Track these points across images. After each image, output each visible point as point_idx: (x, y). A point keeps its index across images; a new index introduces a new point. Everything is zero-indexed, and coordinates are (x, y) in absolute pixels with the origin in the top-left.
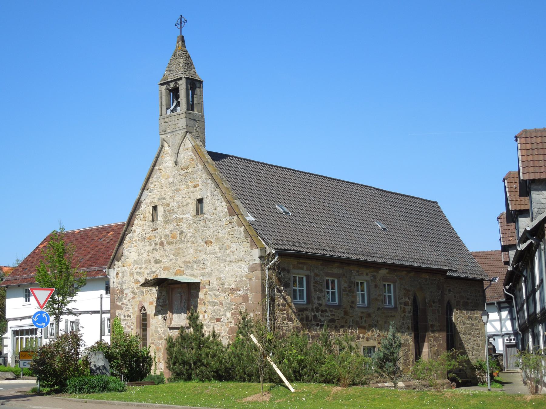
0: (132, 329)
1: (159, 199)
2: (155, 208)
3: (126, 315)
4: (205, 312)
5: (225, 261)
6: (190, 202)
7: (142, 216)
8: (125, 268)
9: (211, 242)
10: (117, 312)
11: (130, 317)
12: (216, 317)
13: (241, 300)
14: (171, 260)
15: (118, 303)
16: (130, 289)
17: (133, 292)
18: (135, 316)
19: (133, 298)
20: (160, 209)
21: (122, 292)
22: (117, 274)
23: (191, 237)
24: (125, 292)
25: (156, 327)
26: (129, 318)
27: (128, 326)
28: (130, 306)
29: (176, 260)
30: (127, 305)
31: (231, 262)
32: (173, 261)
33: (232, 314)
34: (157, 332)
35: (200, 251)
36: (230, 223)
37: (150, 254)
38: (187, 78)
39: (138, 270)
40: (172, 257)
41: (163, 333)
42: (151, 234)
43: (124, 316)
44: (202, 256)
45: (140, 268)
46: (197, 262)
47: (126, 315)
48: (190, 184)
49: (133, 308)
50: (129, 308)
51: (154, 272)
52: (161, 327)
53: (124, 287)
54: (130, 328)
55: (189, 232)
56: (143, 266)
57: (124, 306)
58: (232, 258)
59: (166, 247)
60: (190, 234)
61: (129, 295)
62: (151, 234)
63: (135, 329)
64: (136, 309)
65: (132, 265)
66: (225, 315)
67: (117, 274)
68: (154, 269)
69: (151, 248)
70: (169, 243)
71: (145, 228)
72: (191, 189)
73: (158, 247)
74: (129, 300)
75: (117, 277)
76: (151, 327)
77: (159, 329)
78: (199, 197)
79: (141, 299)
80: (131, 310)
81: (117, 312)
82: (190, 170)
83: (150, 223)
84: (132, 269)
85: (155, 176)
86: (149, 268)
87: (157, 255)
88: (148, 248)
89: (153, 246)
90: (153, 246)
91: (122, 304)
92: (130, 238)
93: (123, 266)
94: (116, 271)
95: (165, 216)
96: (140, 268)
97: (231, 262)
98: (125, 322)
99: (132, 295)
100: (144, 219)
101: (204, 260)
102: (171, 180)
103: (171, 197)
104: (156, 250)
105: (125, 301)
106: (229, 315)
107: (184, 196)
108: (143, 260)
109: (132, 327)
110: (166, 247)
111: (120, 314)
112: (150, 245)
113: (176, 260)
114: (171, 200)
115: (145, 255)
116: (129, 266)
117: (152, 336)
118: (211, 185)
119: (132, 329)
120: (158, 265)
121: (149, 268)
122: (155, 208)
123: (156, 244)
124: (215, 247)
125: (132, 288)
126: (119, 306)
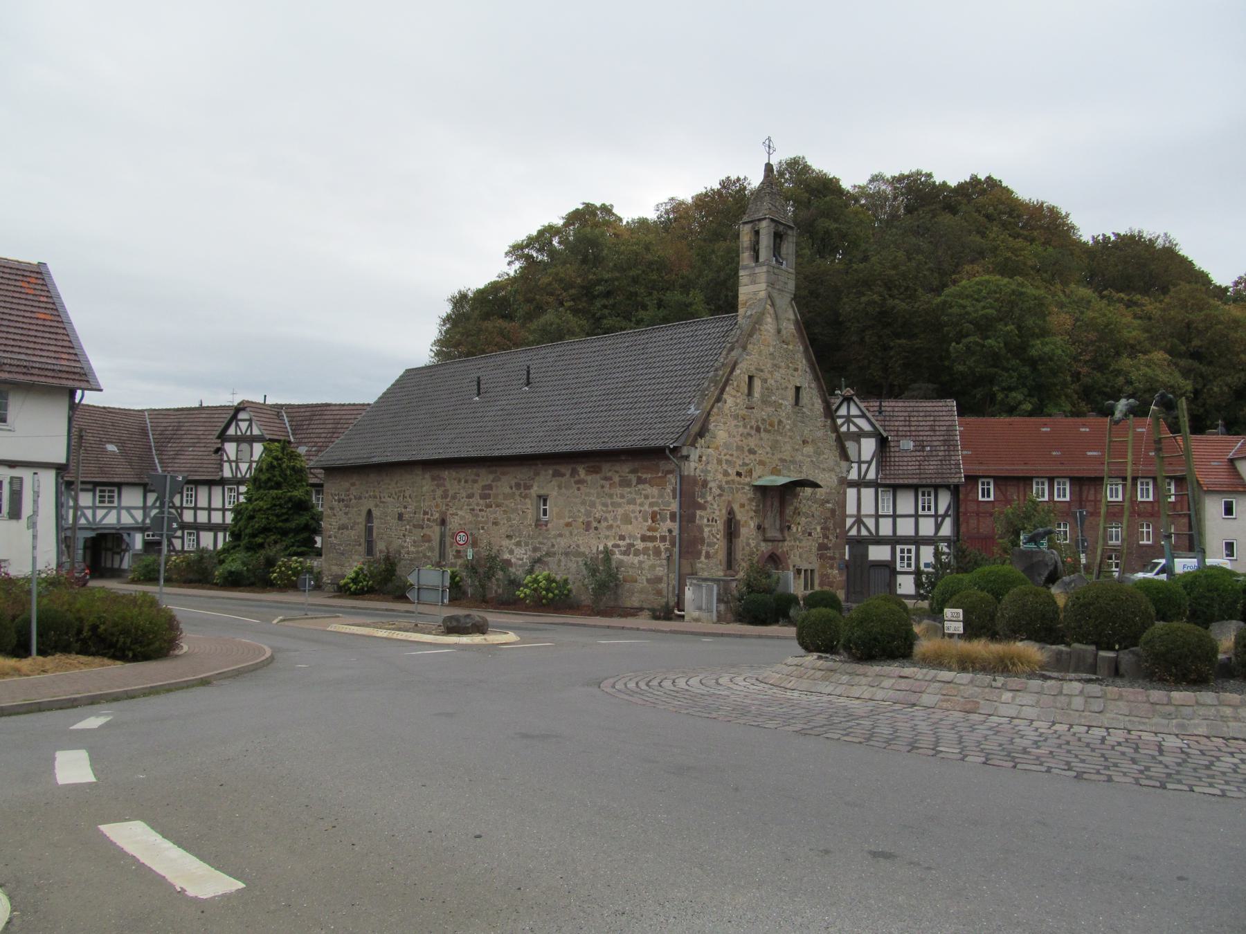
0: (718, 539)
1: (756, 369)
2: (751, 378)
3: (710, 519)
4: (799, 524)
5: (819, 467)
6: (790, 386)
7: (735, 384)
8: (710, 450)
9: (808, 442)
10: (698, 512)
11: (716, 522)
12: (808, 531)
13: (829, 515)
14: (767, 453)
15: (699, 500)
16: (717, 482)
17: (720, 487)
18: (723, 521)
19: (720, 495)
20: (757, 383)
21: (705, 484)
22: (700, 457)
23: (789, 430)
24: (709, 486)
25: (748, 539)
26: (714, 523)
27: (713, 534)
28: (715, 506)
29: (773, 454)
30: (712, 505)
31: (824, 470)
32: (769, 455)
33: (822, 529)
34: (748, 544)
35: (797, 450)
36: (825, 426)
37: (743, 439)
38: (772, 220)
39: (728, 457)
40: (768, 449)
41: (755, 547)
42: (744, 412)
43: (708, 520)
44: (799, 458)
45: (732, 455)
46: (793, 462)
47: (710, 519)
48: (790, 365)
49: (720, 510)
50: (715, 509)
51: (747, 465)
52: (753, 539)
53: (709, 478)
54: (716, 537)
55: (788, 424)
56: (735, 453)
57: (709, 506)
58: (825, 466)
59: (763, 434)
60: (788, 427)
61: (714, 490)
62: (744, 412)
63: (722, 539)
64: (724, 511)
65: (720, 449)
66: (815, 529)
67: (700, 457)
68: (747, 461)
69: (746, 431)
70: (766, 431)
71: (738, 401)
72: (791, 371)
73: (753, 432)
74: (714, 498)
75: (700, 461)
76: (741, 538)
77: (751, 541)
78: (798, 385)
79: (730, 499)
80: (717, 513)
81: (698, 512)
82: (791, 347)
83: (745, 397)
84: (720, 455)
85: (755, 337)
86: (741, 457)
87: (752, 442)
88: (741, 430)
89: (748, 430)
90: (748, 430)
91: (705, 502)
92: (719, 408)
93: (708, 447)
94: (698, 452)
95: (762, 395)
96: (732, 455)
97: (824, 470)
98: (709, 529)
99: (718, 492)
100: (737, 389)
101: (800, 461)
102: (771, 349)
103: (771, 373)
104: (752, 436)
105: (709, 498)
106: (819, 529)
107: (784, 376)
108: (735, 444)
109: (718, 536)
110: (763, 434)
111: (702, 517)
112: (745, 426)
113: (773, 454)
114: (769, 376)
115: (738, 438)
116: (717, 448)
117: (743, 549)
118: (809, 376)
119: (718, 539)
120: (752, 456)
121: (741, 457)
122: (751, 378)
123: (752, 427)
124: (809, 449)
125: (720, 481)
126: (700, 503)
